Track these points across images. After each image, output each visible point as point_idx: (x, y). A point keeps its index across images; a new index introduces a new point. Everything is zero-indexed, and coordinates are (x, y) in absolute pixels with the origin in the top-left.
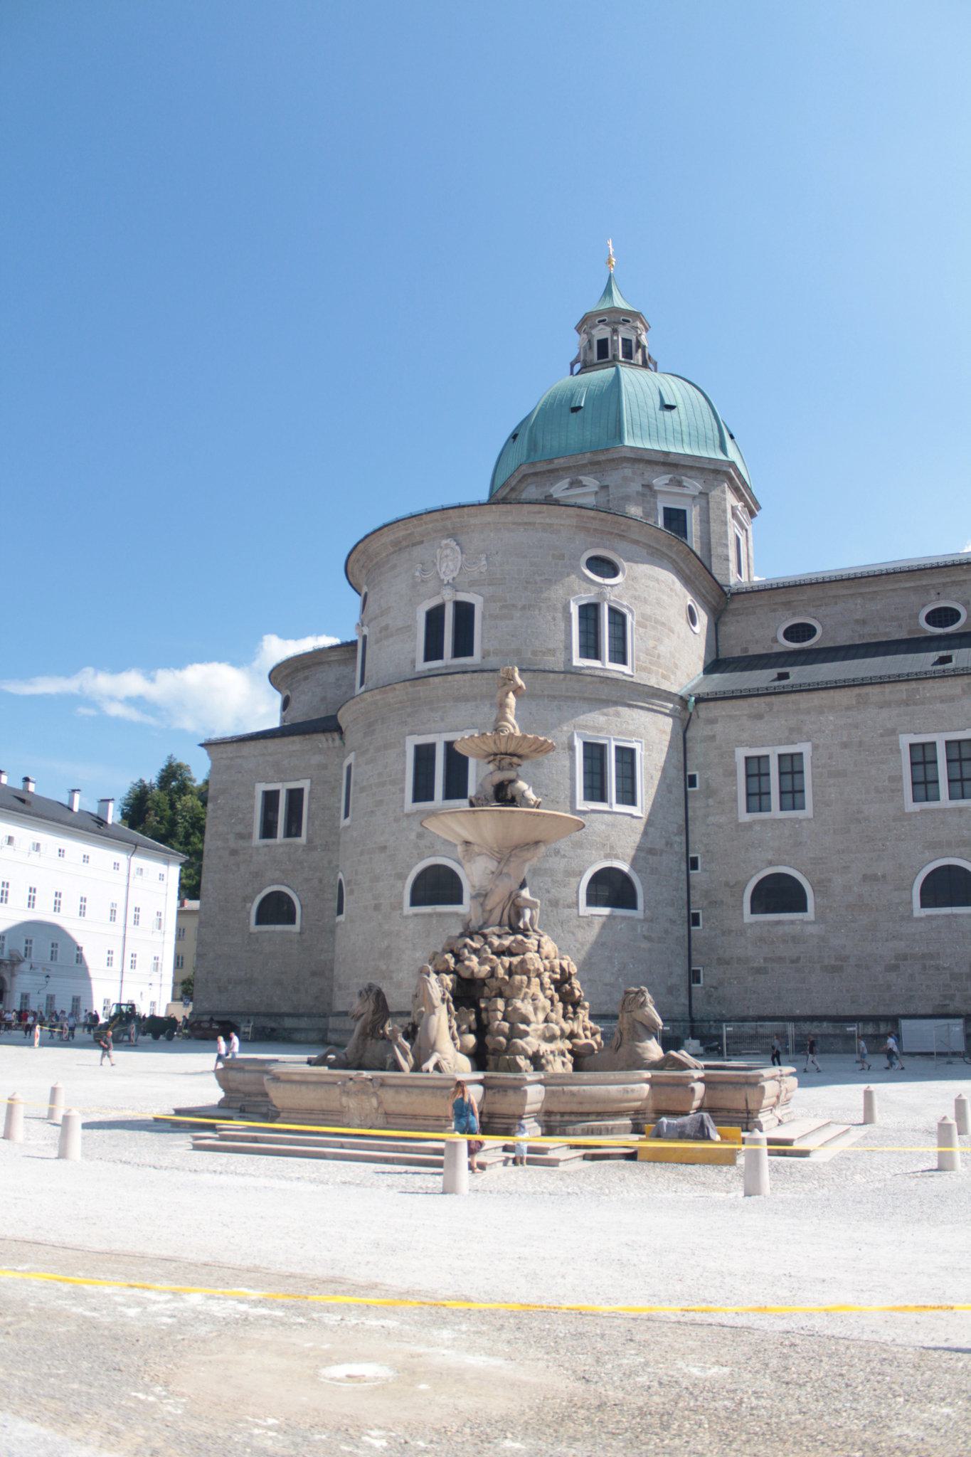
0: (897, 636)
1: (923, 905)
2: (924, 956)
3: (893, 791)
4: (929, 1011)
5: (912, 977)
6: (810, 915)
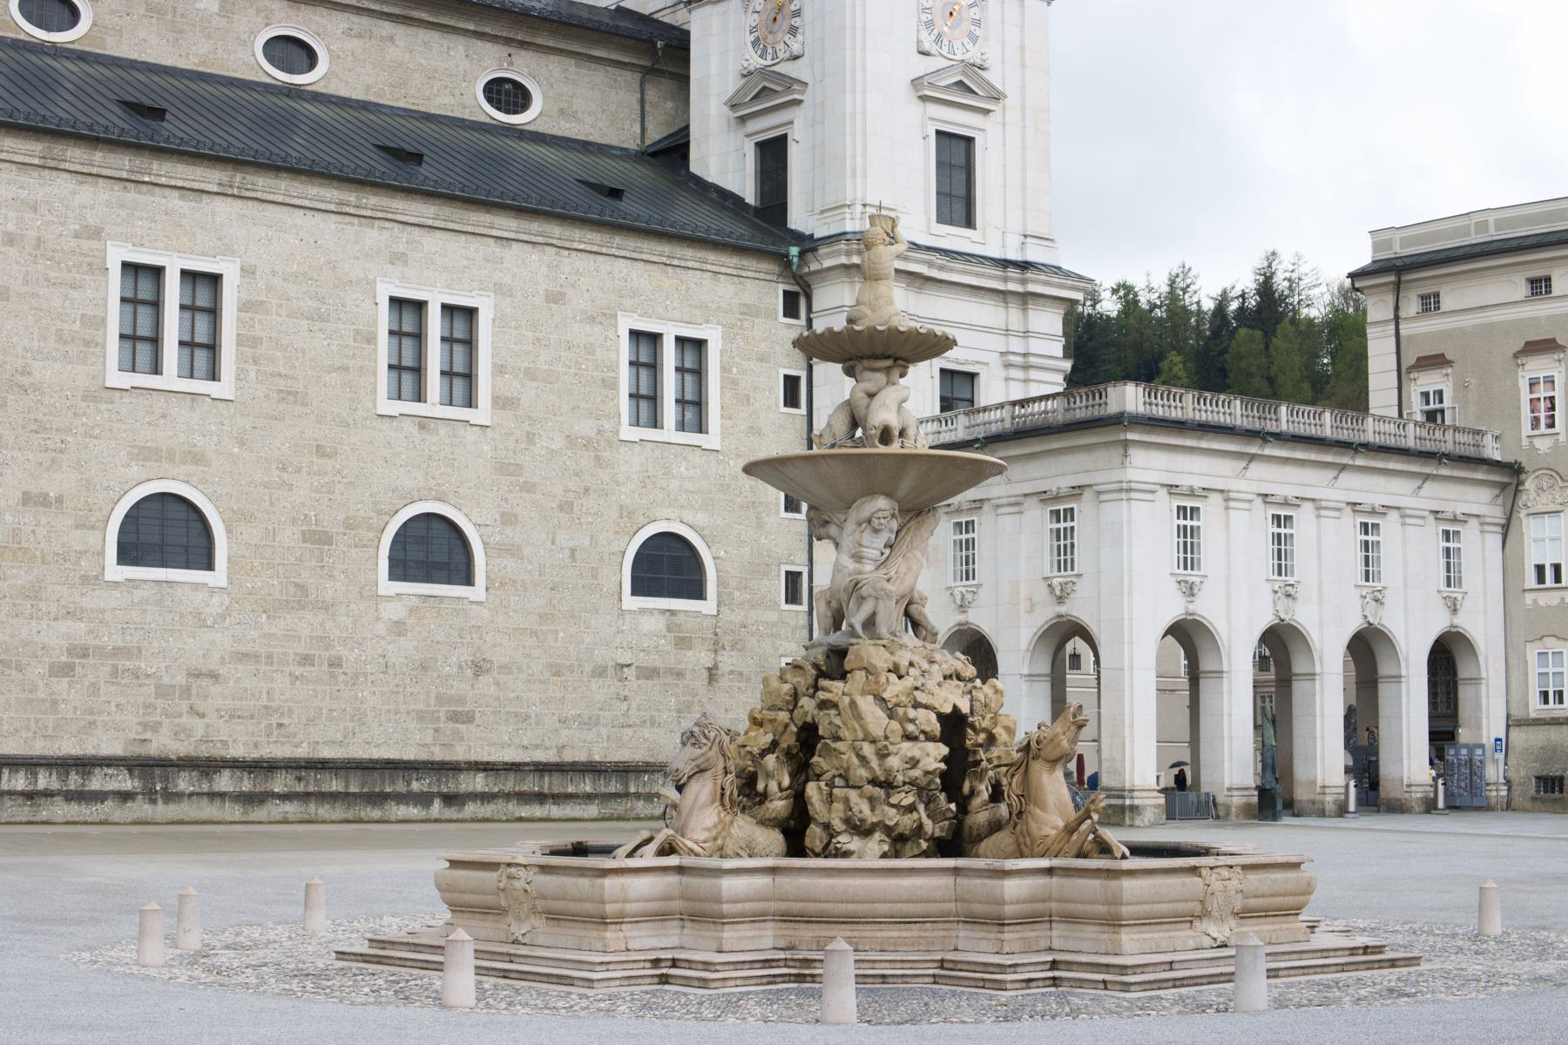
2: (117, 652)
3: (87, 344)
5: (94, 689)
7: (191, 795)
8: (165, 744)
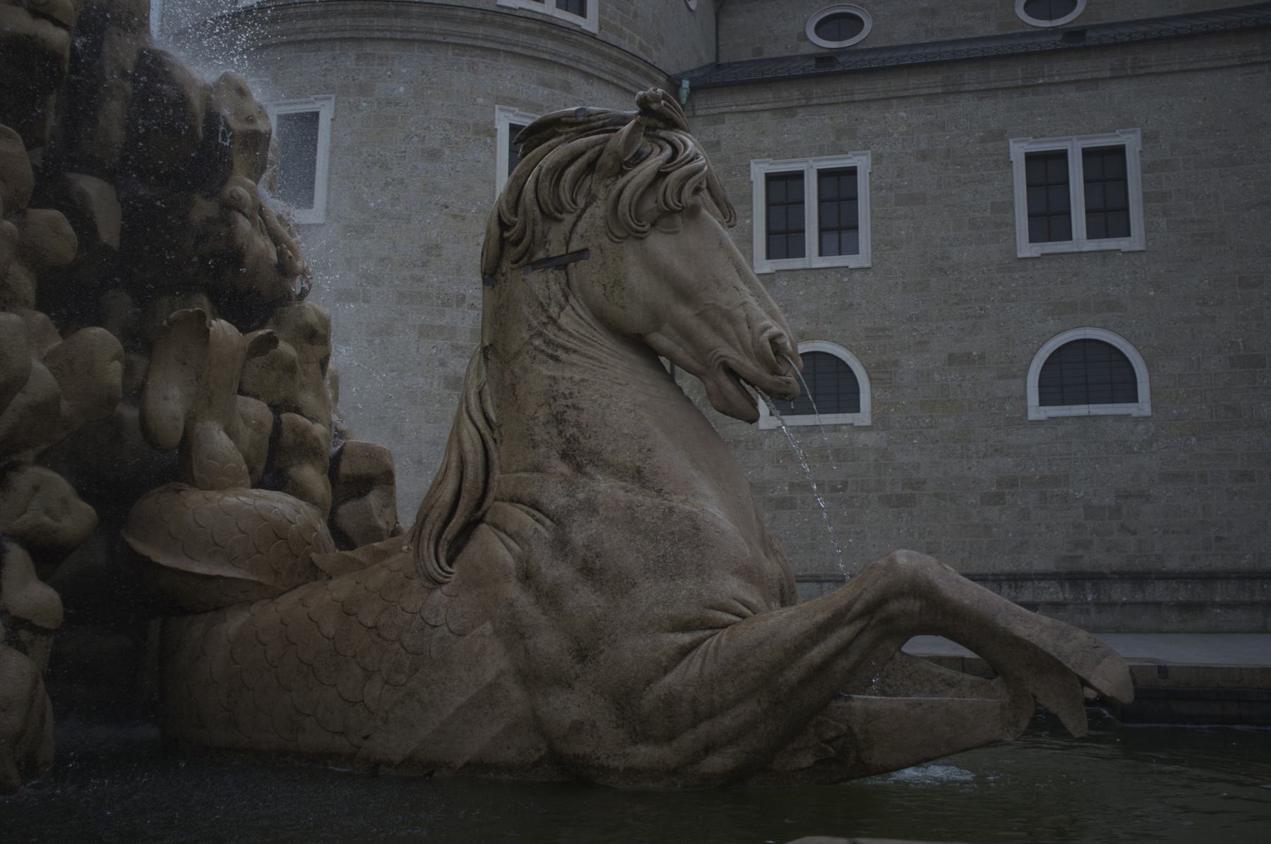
0: (981, 32)
1: (1043, 402)
4: (1051, 567)
6: (864, 417)
7: (1124, 604)
8: (1096, 558)
